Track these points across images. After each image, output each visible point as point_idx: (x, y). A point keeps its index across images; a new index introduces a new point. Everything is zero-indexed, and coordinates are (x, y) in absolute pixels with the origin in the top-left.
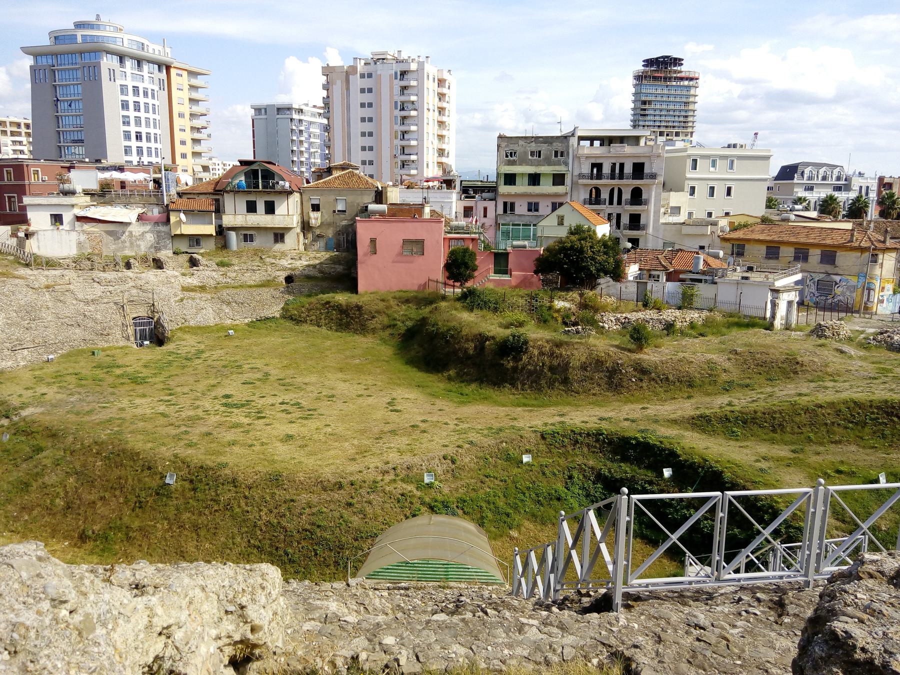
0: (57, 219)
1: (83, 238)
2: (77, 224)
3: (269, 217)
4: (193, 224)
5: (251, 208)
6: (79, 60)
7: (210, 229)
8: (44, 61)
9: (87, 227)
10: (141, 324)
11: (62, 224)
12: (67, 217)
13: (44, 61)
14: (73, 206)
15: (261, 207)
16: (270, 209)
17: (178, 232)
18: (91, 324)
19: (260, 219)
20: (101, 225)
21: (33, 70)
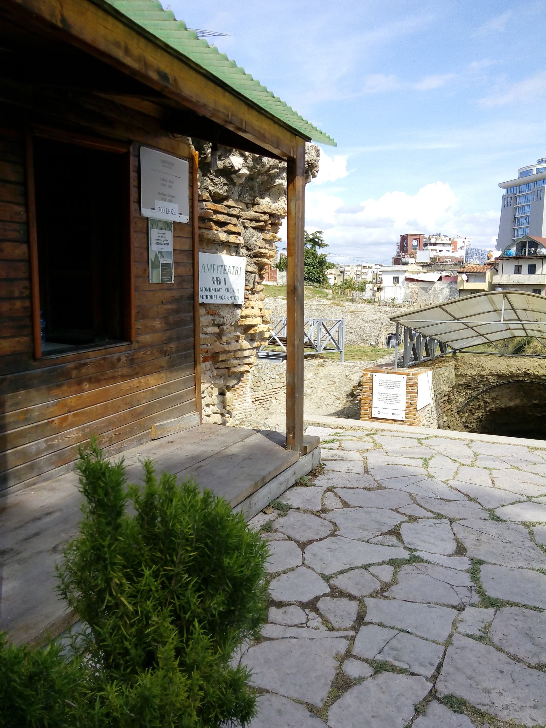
0: (396, 279)
1: (408, 291)
2: (406, 282)
3: (532, 276)
4: (475, 282)
5: (518, 270)
6: (533, 187)
7: (484, 286)
8: (511, 191)
9: (411, 284)
10: (393, 338)
11: (398, 283)
12: (402, 278)
13: (511, 191)
14: (405, 271)
15: (525, 269)
16: (532, 270)
17: (462, 288)
18: (362, 333)
19: (524, 278)
20: (418, 283)
21: (504, 199)
